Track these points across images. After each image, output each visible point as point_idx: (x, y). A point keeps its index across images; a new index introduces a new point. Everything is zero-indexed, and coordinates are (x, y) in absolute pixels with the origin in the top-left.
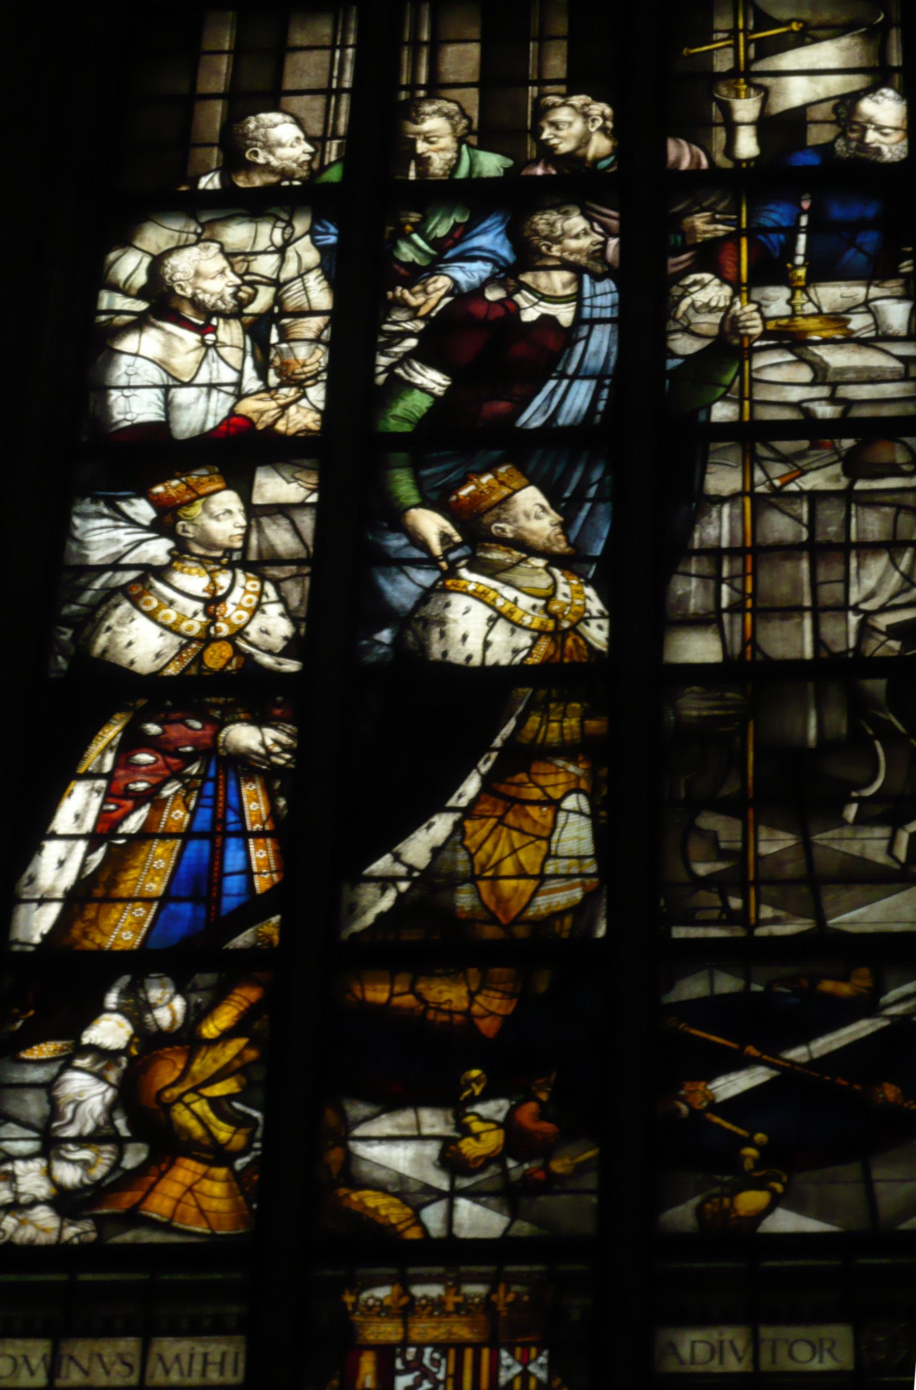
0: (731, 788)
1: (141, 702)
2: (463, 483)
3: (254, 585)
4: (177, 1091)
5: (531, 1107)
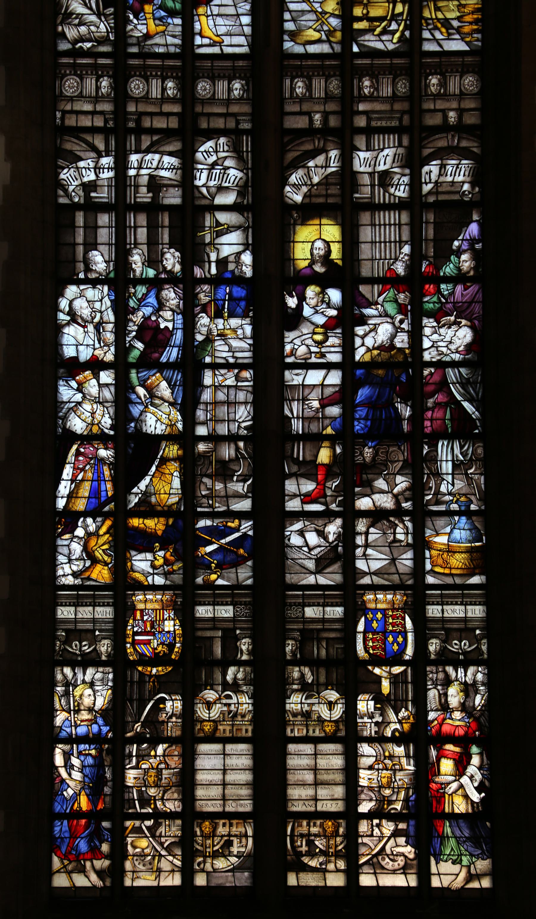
0: (209, 471)
1: (79, 442)
2: (148, 379)
3: (102, 408)
4: (95, 548)
5: (169, 553)
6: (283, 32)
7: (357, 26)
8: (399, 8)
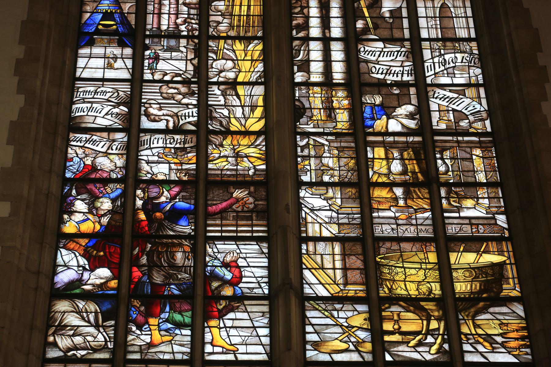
6: (305, 342)
7: (387, 338)
8: (434, 325)
